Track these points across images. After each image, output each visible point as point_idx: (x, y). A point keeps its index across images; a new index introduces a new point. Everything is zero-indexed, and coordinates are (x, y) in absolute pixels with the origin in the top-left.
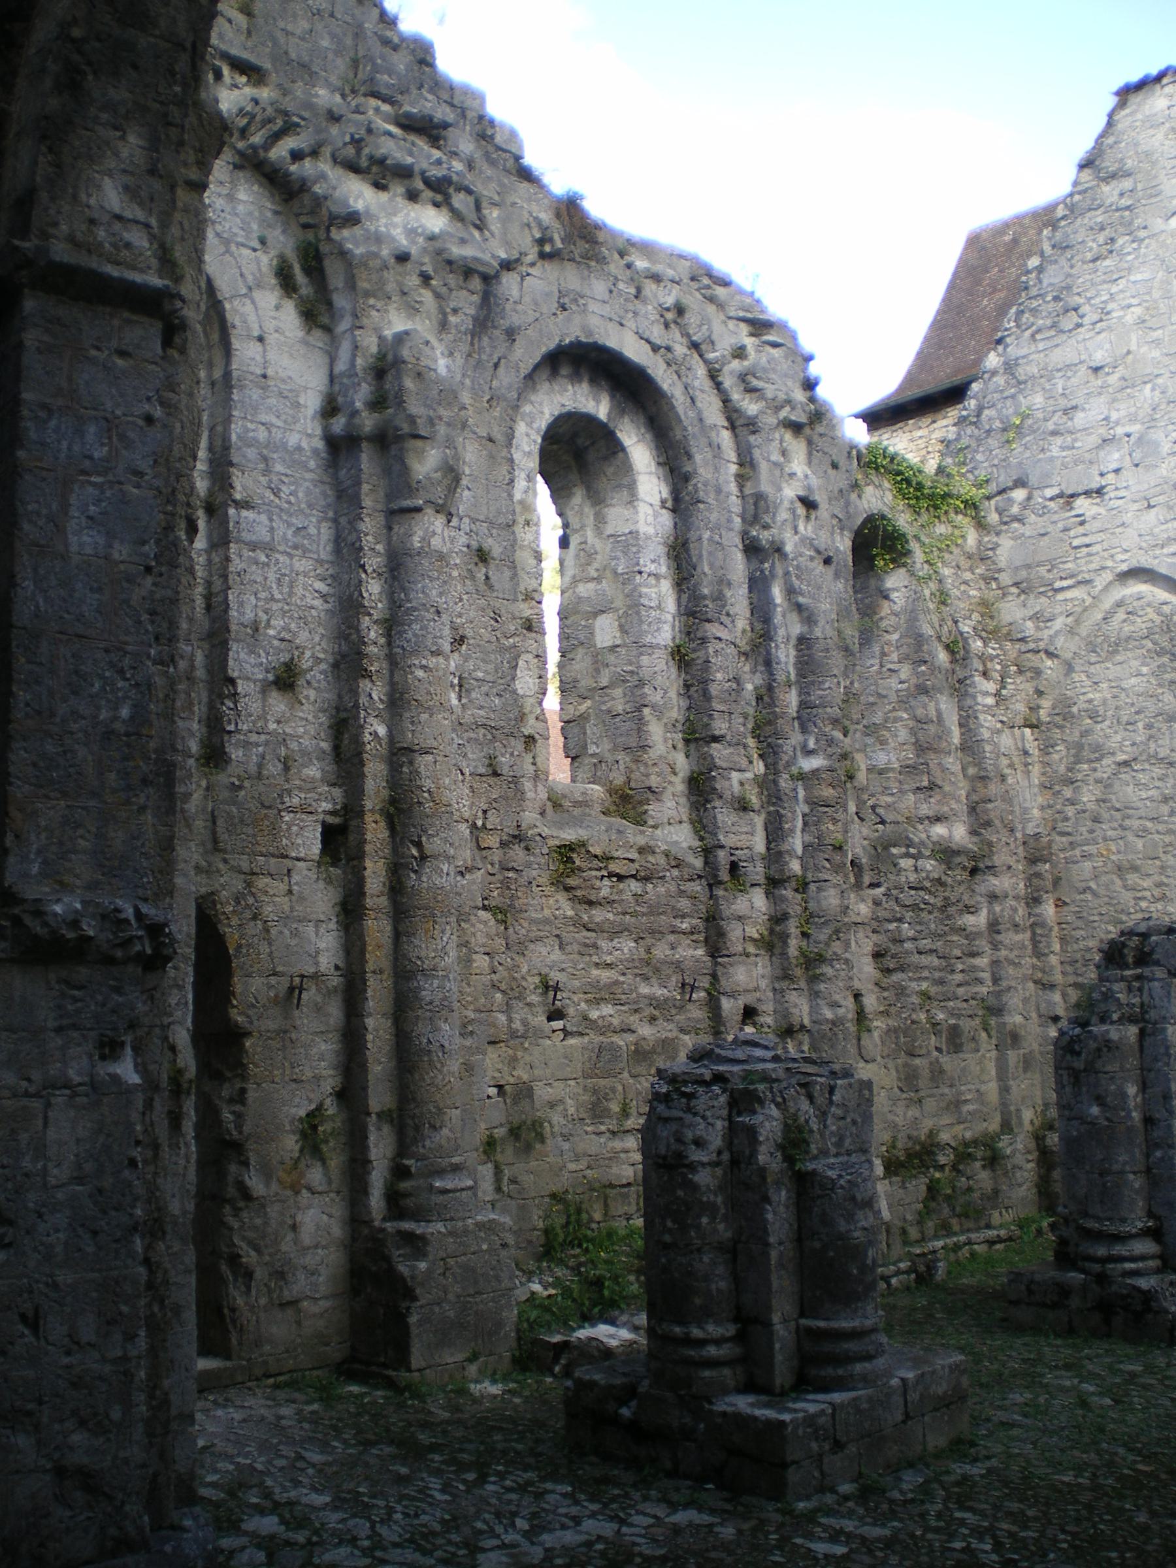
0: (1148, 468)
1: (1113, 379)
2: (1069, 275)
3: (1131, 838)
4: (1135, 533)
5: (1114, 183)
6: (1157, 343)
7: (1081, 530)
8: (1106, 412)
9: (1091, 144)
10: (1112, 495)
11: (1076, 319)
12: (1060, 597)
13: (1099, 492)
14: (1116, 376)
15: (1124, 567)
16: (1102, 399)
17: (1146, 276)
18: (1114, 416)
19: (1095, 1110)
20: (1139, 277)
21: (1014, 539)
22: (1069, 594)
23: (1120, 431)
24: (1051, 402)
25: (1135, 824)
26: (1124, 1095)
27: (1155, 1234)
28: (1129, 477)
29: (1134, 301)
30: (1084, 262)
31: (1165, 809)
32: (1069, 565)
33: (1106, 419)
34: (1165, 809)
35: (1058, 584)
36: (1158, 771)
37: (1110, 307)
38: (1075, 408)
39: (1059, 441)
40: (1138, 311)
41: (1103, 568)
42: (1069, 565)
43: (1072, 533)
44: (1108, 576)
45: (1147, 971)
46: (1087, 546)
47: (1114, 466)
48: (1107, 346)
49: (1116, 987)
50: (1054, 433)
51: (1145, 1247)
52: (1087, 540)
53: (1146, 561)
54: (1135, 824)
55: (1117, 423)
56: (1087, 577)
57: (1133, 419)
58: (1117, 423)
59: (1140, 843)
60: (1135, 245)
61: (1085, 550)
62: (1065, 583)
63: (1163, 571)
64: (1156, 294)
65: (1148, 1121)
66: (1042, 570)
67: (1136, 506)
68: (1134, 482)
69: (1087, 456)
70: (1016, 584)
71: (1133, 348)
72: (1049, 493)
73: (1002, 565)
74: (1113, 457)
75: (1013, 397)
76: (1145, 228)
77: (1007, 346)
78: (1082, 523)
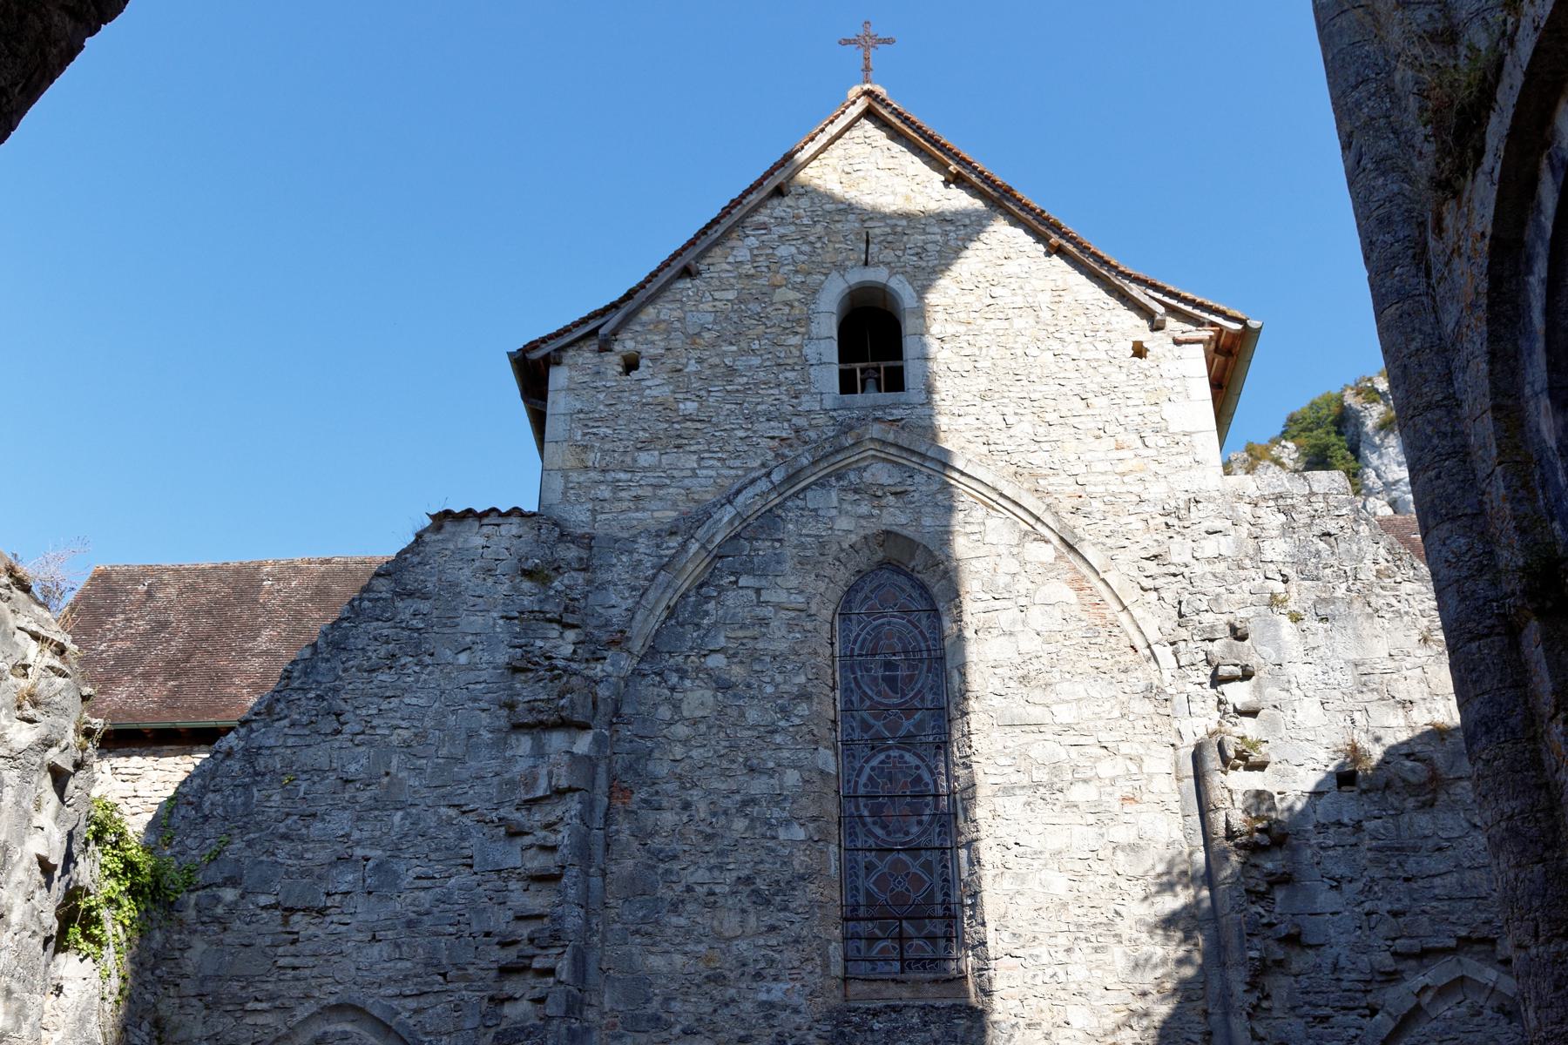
0: (381, 898)
1: (364, 797)
2: (341, 679)
4: (353, 966)
5: (409, 601)
6: (420, 771)
7: (292, 949)
8: (347, 829)
9: (392, 554)
10: (335, 919)
11: (336, 725)
12: (249, 1020)
13: (322, 912)
14: (368, 794)
15: (333, 1000)
16: (346, 814)
17: (422, 702)
18: (356, 835)
20: (414, 701)
21: (210, 943)
22: (261, 1020)
23: (359, 852)
24: (289, 803)
28: (360, 903)
29: (404, 724)
30: (359, 670)
32: (270, 986)
33: (347, 836)
35: (250, 1006)
37: (374, 723)
38: (314, 815)
39: (287, 846)
40: (406, 734)
41: (307, 997)
42: (270, 986)
43: (280, 950)
44: (309, 1007)
46: (294, 968)
47: (343, 888)
48: (364, 761)
50: (284, 837)
52: (296, 962)
53: (356, 995)
55: (358, 843)
56: (287, 1004)
57: (375, 843)
58: (358, 843)
60: (417, 669)
61: (291, 973)
62: (259, 1006)
63: (376, 1013)
64: (428, 723)
66: (236, 986)
67: (360, 936)
68: (364, 911)
69: (317, 871)
70: (200, 996)
71: (393, 771)
72: (263, 900)
73: (189, 970)
74: (348, 878)
75: (246, 786)
76: (432, 655)
77: (252, 731)
78: (294, 942)
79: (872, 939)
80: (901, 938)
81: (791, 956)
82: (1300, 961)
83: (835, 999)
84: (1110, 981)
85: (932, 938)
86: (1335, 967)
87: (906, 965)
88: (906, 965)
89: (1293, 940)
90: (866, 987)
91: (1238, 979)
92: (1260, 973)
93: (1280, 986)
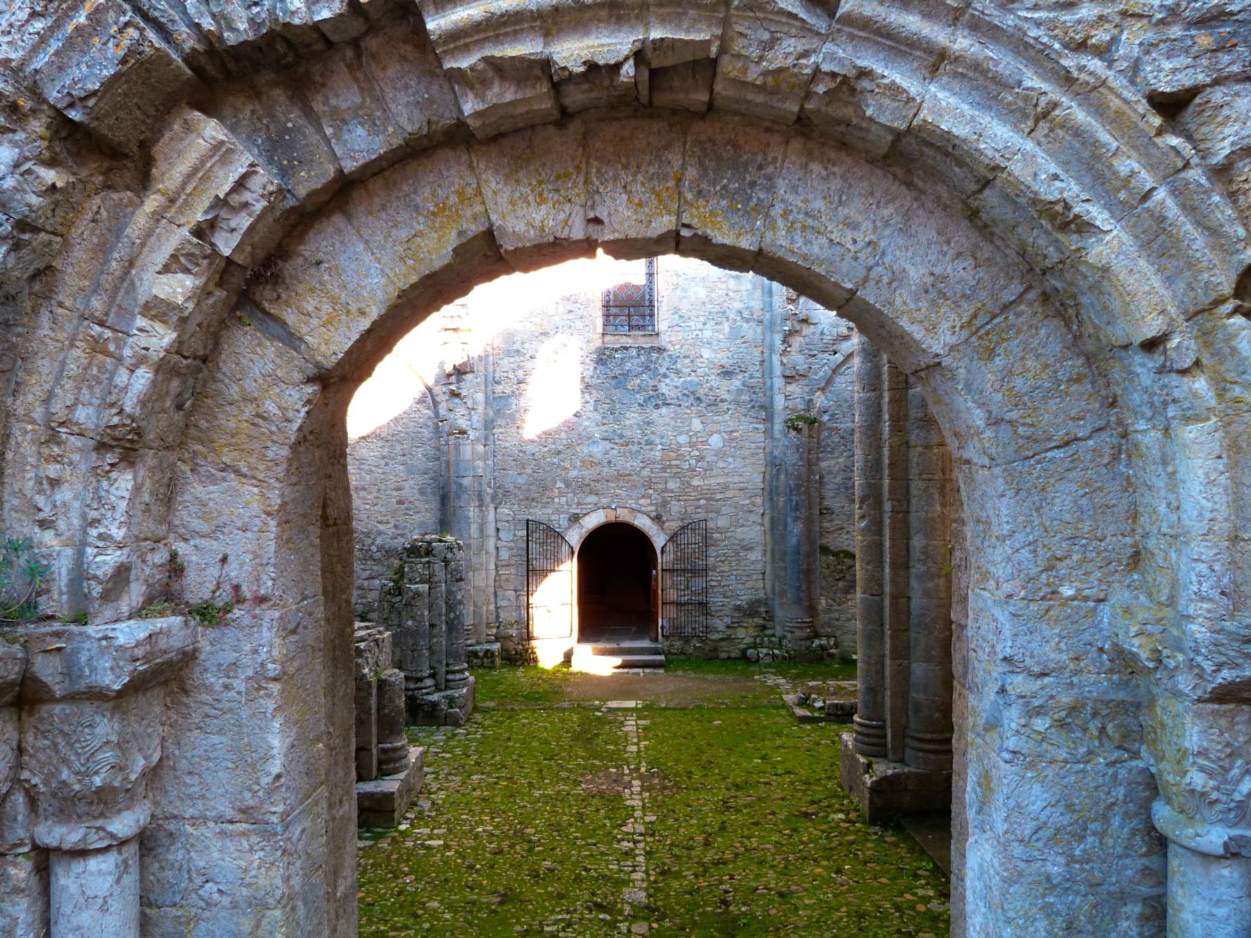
3: (363, 474)
19: (410, 623)
25: (366, 467)
26: (422, 615)
27: (433, 676)
31: (383, 462)
34: (383, 462)
36: (380, 444)
45: (431, 559)
49: (420, 566)
51: (429, 682)
54: (366, 467)
59: (368, 477)
65: (432, 626)
79: (616, 316)
80: (629, 315)
81: (579, 324)
82: (807, 330)
83: (598, 343)
84: (721, 337)
85: (643, 316)
86: (822, 333)
87: (631, 327)
88: (631, 327)
89: (805, 321)
90: (612, 338)
91: (778, 339)
92: (787, 337)
93: (797, 341)
